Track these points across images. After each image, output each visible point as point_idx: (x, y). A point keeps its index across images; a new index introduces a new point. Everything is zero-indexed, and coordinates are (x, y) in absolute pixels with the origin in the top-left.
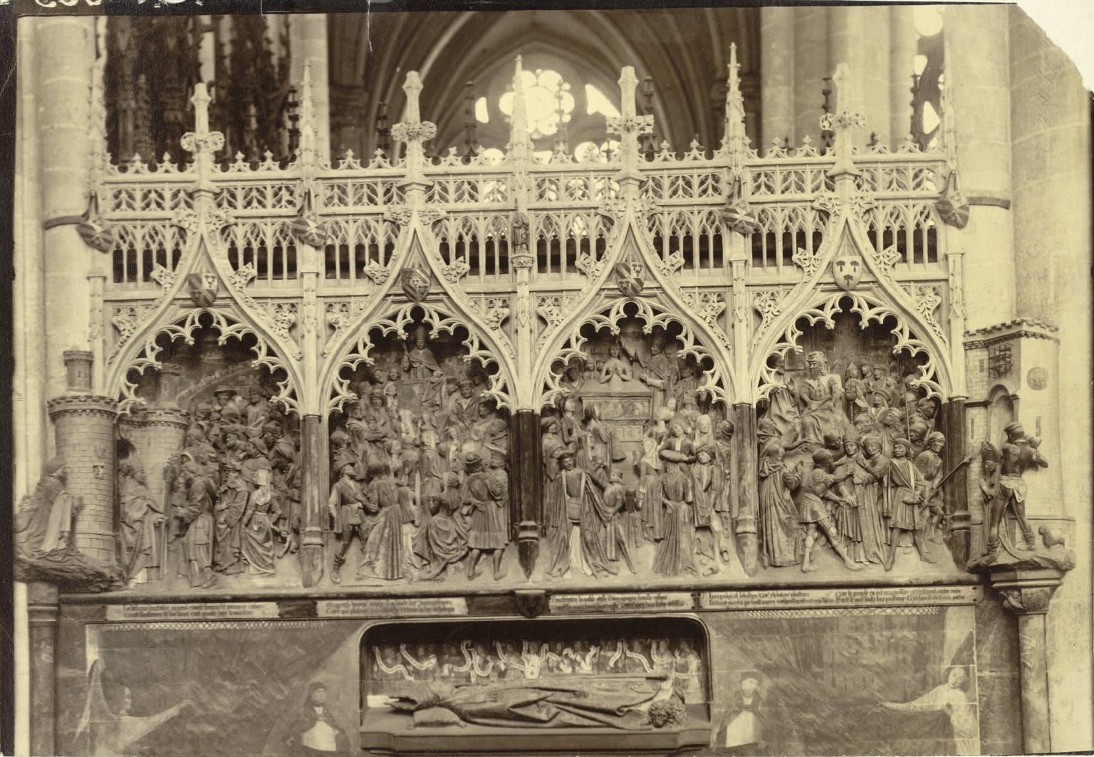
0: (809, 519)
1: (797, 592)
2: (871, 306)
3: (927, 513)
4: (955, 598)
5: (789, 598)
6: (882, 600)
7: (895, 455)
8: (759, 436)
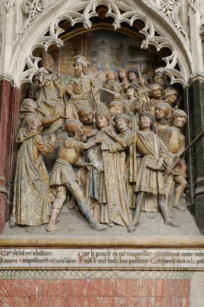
0: (59, 183)
1: (39, 250)
2: (122, 12)
3: (170, 181)
4: (198, 262)
5: (31, 257)
6: (125, 261)
7: (141, 129)
8: (21, 112)
